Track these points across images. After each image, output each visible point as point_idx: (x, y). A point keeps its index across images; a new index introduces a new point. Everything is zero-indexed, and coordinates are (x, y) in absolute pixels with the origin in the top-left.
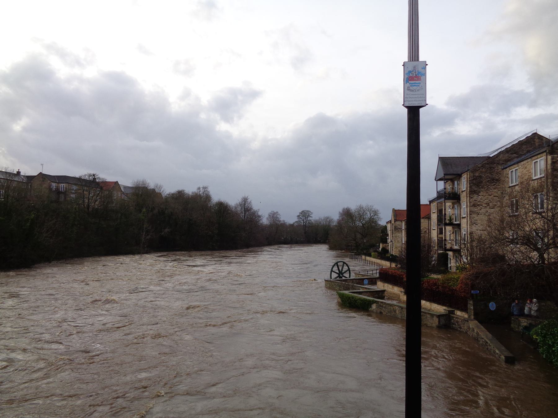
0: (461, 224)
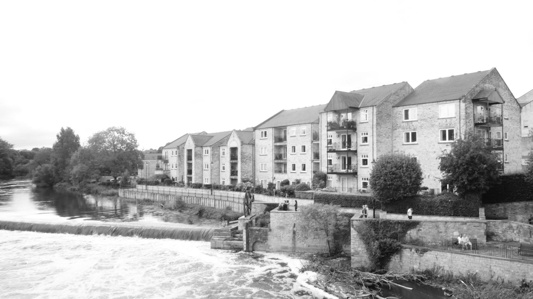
0: (358, 151)
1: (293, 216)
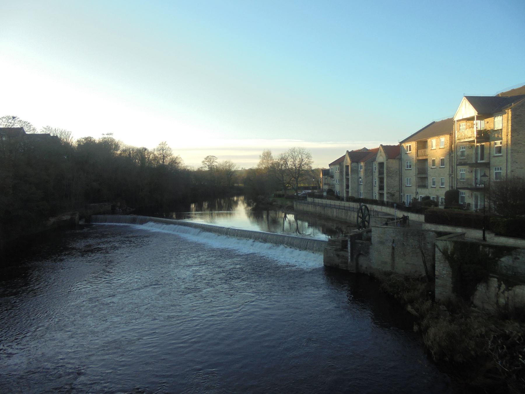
0: (491, 163)
1: (392, 231)
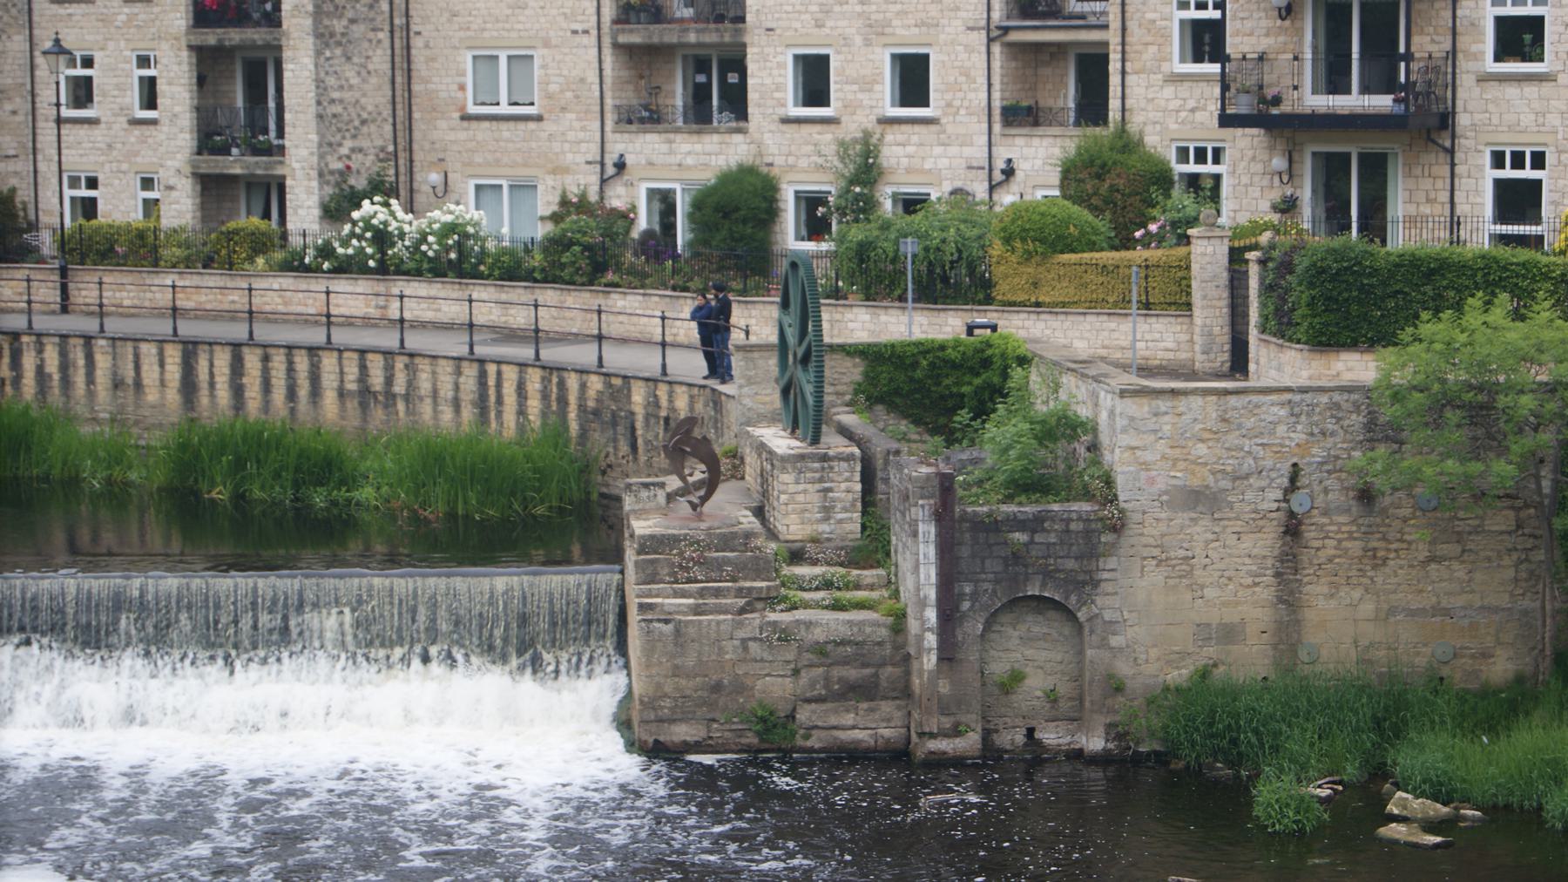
1: (1283, 412)
